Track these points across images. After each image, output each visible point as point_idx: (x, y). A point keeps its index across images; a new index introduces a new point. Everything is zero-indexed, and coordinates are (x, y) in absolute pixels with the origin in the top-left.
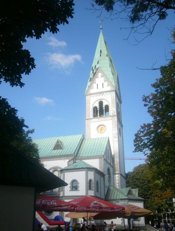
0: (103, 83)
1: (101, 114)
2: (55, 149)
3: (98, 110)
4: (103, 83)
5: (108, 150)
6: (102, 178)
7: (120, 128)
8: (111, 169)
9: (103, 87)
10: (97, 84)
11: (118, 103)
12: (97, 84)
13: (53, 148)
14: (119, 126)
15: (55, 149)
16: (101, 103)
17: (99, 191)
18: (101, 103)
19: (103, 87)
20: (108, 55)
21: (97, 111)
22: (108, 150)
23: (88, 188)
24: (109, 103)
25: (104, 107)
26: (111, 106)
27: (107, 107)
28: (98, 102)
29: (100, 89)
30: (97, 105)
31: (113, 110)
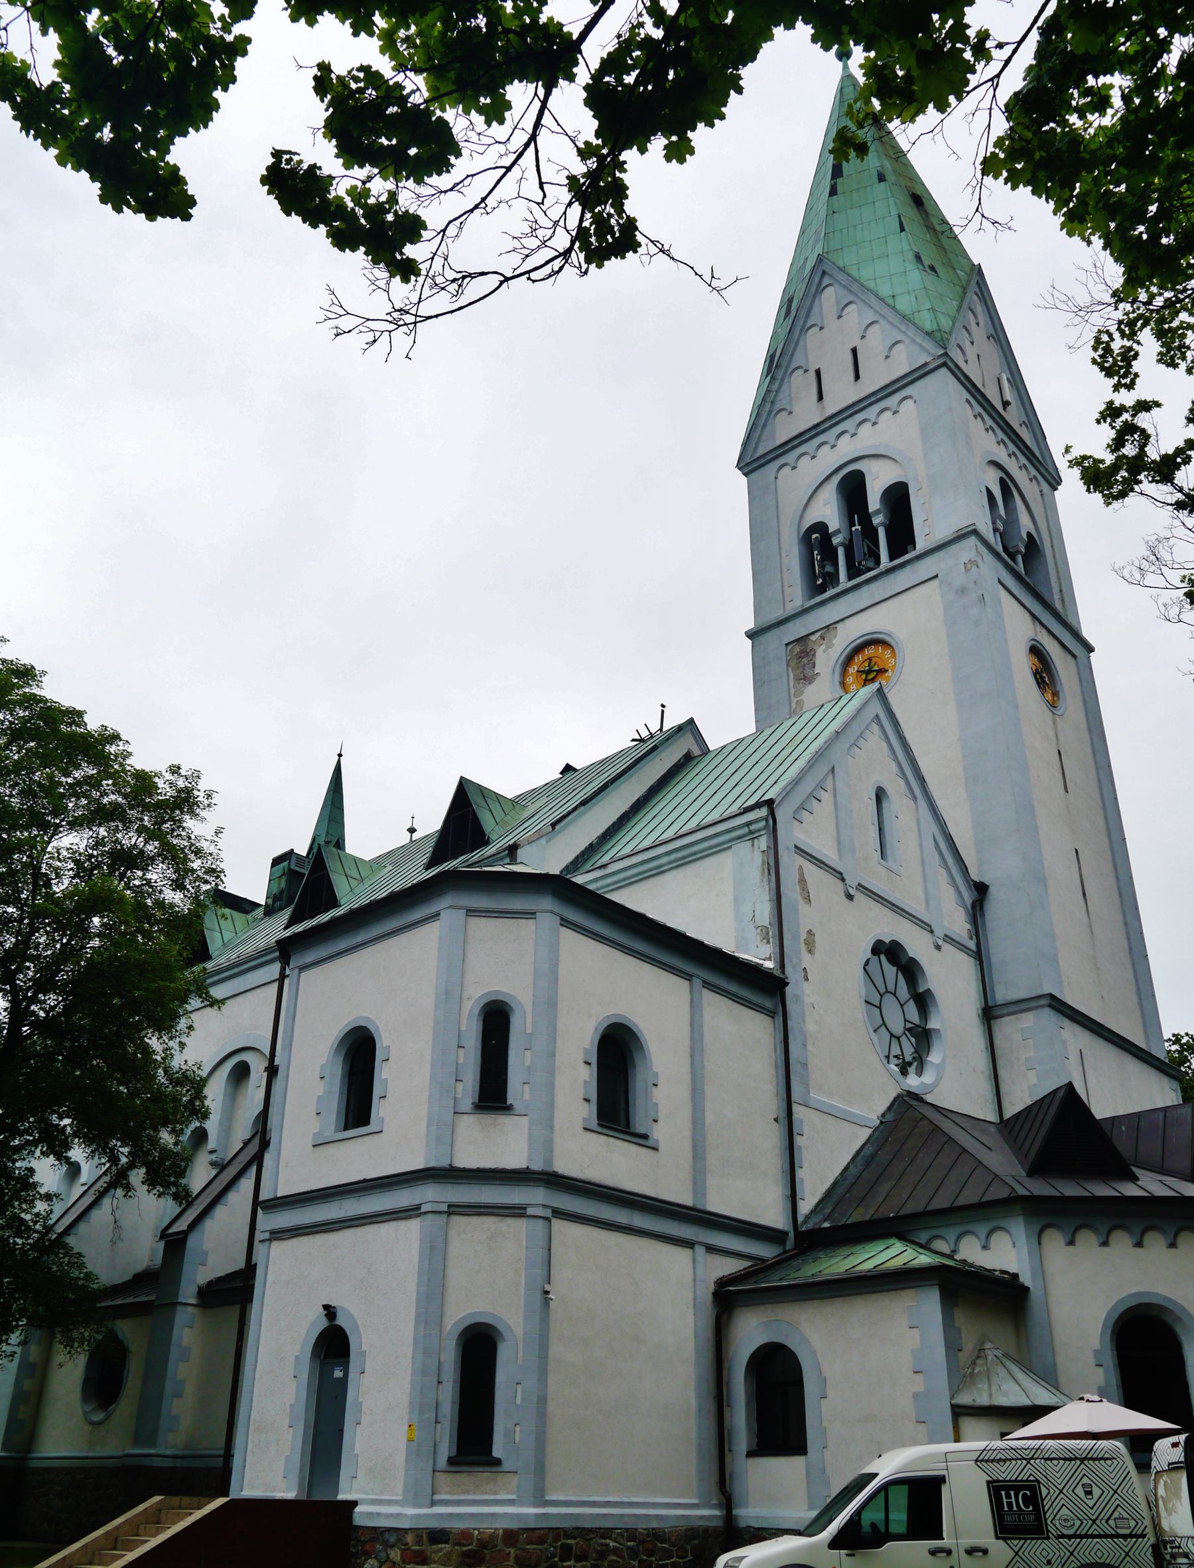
0: (854, 351)
1: (862, 563)
3: (836, 540)
4: (854, 351)
7: (1036, 651)
8: (951, 981)
9: (857, 377)
10: (818, 373)
11: (995, 464)
12: (818, 373)
16: (853, 489)
18: (853, 489)
19: (857, 377)
20: (891, 177)
21: (829, 553)
25: (874, 501)
28: (830, 494)
29: (841, 393)
30: (828, 510)
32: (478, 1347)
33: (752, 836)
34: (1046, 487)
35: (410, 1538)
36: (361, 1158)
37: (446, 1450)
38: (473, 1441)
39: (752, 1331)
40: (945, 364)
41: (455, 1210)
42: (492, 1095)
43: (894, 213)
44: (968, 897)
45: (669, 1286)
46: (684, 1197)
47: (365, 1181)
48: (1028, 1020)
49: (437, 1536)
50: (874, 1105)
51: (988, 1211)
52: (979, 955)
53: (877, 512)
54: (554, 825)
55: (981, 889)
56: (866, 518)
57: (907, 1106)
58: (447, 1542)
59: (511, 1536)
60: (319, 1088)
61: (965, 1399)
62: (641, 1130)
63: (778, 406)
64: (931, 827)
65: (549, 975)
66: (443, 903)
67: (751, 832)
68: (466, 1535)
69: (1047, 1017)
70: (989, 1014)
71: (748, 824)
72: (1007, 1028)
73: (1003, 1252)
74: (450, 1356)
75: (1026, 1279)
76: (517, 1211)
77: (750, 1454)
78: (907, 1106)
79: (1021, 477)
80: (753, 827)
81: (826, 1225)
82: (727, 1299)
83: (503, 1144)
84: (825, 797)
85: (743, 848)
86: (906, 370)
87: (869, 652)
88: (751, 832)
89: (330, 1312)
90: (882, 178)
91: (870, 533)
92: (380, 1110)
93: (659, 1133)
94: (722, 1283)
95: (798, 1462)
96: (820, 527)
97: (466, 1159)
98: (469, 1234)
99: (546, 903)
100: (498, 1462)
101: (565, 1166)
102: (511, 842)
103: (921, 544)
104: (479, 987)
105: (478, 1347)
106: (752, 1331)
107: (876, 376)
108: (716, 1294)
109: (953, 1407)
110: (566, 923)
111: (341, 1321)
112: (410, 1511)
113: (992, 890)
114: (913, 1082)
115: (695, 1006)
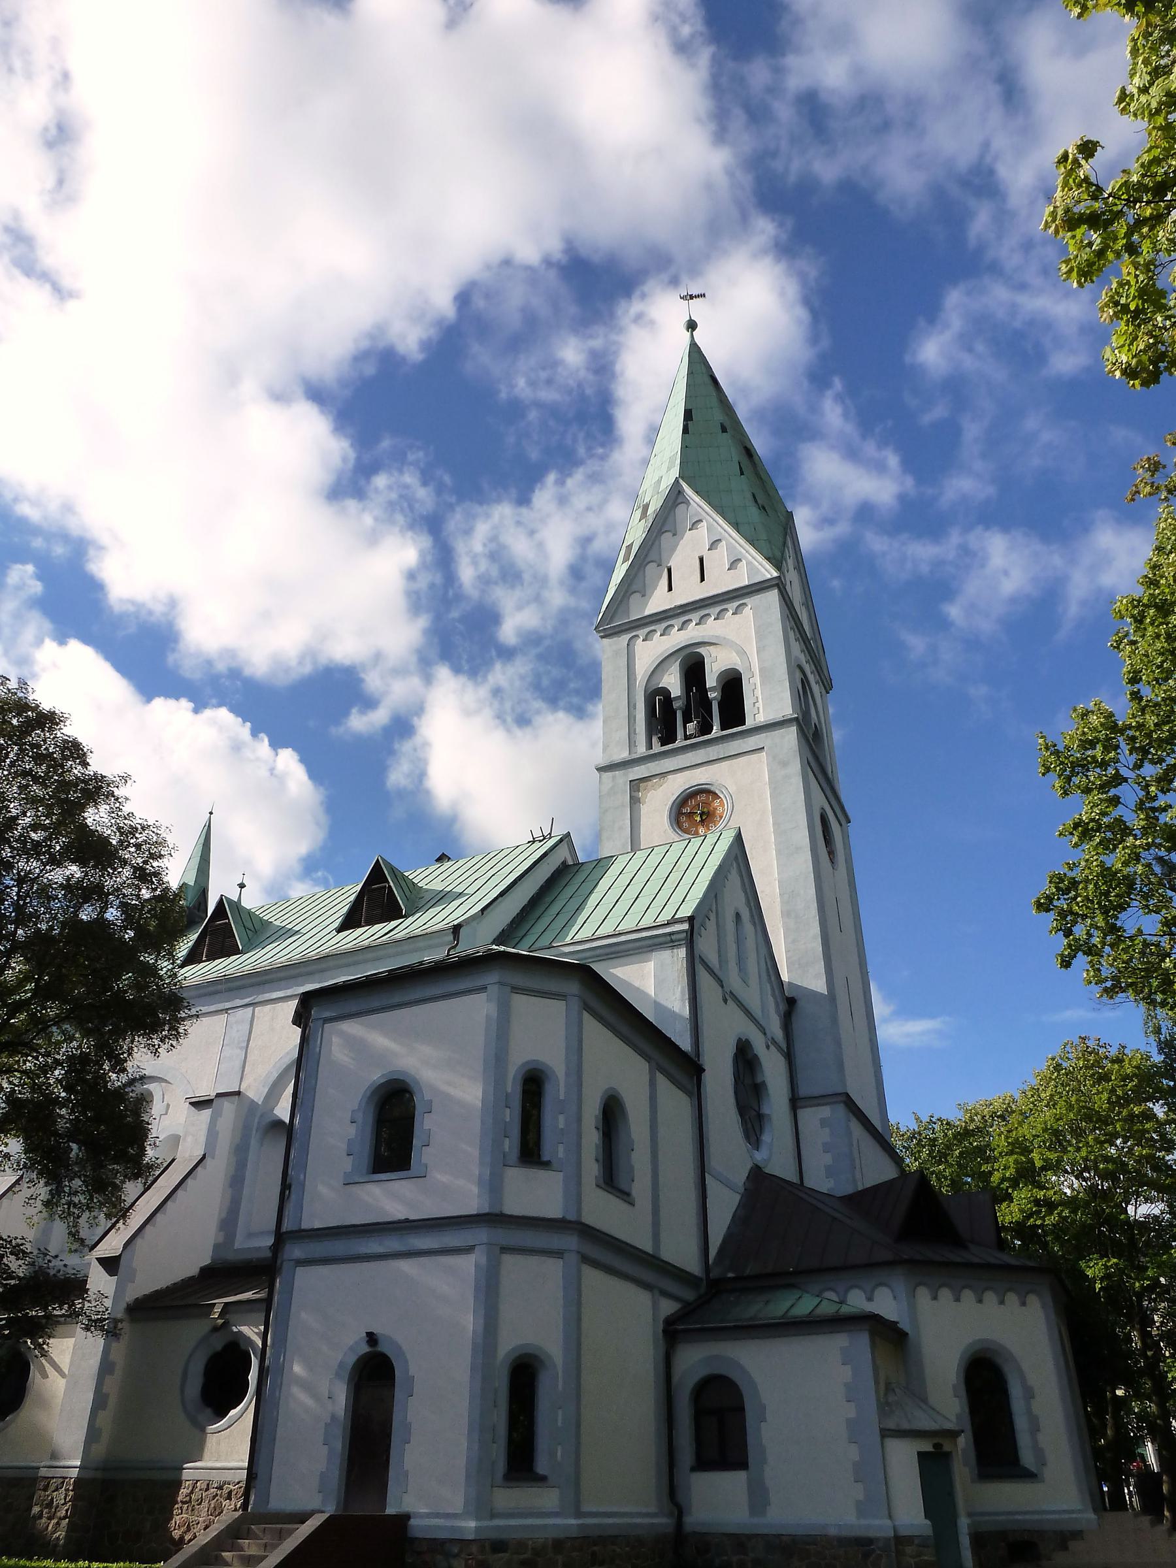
0: (701, 560)
2: (350, 922)
3: (676, 705)
4: (701, 560)
5: (738, 915)
6: (674, 1103)
9: (702, 579)
11: (800, 667)
13: (336, 925)
14: (820, 800)
15: (350, 922)
16: (694, 670)
17: (640, 1188)
18: (694, 670)
19: (702, 579)
22: (738, 915)
23: (511, 1145)
24: (742, 653)
25: (711, 681)
26: (757, 679)
27: (733, 684)
29: (688, 590)
30: (673, 682)
31: (768, 698)
32: (524, 1376)
33: (668, 942)
34: (824, 692)
35: (474, 1549)
36: (390, 1199)
37: (501, 1467)
38: (520, 1460)
39: (694, 1360)
40: (777, 585)
41: (505, 1249)
42: (530, 1153)
43: (736, 459)
44: (783, 1007)
45: (627, 1319)
46: (645, 1244)
47: (407, 1220)
48: (825, 1112)
49: (498, 1546)
50: (740, 1177)
51: (867, 1268)
52: (789, 1056)
53: (713, 689)
54: (483, 910)
55: (791, 1002)
56: (703, 690)
57: (757, 1174)
58: (505, 1551)
59: (558, 1545)
60: (352, 1131)
61: (891, 1424)
62: (627, 1190)
63: (634, 587)
64: (763, 951)
65: (576, 1049)
66: (491, 978)
67: (672, 941)
68: (521, 1545)
69: (841, 1111)
70: (796, 1102)
71: (671, 934)
72: (804, 1114)
73: (886, 1303)
74: (502, 1384)
75: (905, 1325)
76: (558, 1254)
77: (693, 1469)
78: (757, 1174)
79: (812, 678)
80: (673, 937)
81: (730, 1275)
82: (673, 1333)
83: (537, 1194)
84: (713, 916)
85: (665, 955)
86: (747, 583)
87: (703, 797)
88: (672, 941)
89: (372, 1338)
90: (724, 430)
91: (707, 704)
92: (422, 1155)
93: (634, 1193)
94: (669, 1322)
95: (741, 1476)
96: (665, 692)
97: (512, 1207)
98: (518, 1271)
99: (573, 987)
100: (543, 1479)
101: (589, 1219)
102: (456, 923)
103: (750, 722)
104: (521, 1056)
105: (524, 1376)
106: (694, 1360)
107: (721, 581)
108: (665, 1332)
109: (881, 1430)
110: (587, 1007)
111: (383, 1348)
112: (472, 1524)
113: (801, 1004)
114: (760, 1156)
115: (652, 1083)
